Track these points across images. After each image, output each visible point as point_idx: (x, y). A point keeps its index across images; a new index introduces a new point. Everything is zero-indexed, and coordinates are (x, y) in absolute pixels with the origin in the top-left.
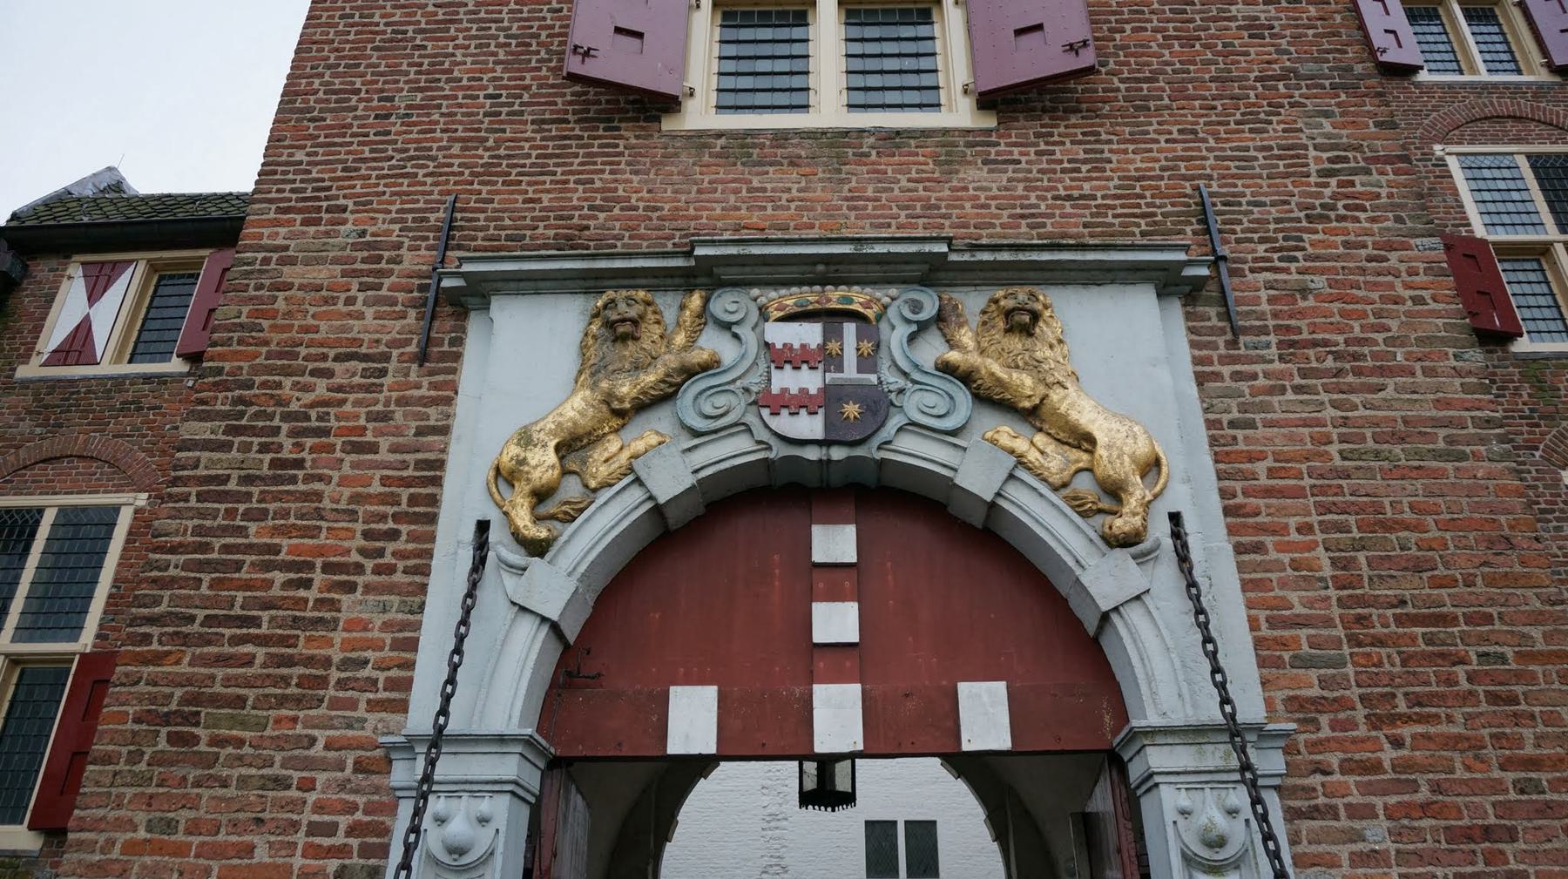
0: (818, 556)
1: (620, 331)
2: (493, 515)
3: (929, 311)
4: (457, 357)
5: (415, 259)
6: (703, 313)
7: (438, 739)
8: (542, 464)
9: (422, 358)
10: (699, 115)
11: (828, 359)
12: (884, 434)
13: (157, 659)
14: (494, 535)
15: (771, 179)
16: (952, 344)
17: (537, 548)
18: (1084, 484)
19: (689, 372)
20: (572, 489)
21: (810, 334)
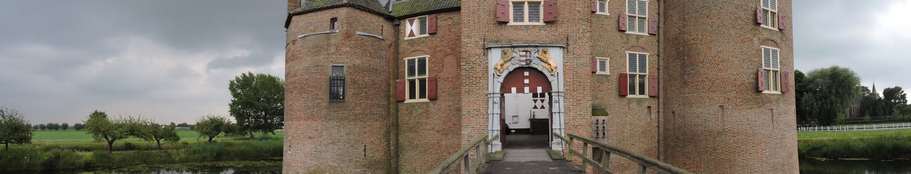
0: (525, 75)
1: (505, 54)
2: (495, 73)
3: (536, 50)
4: (487, 55)
5: (481, 43)
6: (513, 51)
7: (493, 93)
8: (499, 67)
9: (484, 55)
10: (512, 23)
11: (526, 56)
12: (532, 64)
13: (464, 87)
14: (495, 74)
15: (520, 32)
16: (539, 55)
17: (499, 76)
18: (550, 69)
19: (512, 58)
20: (502, 70)
21: (524, 53)
